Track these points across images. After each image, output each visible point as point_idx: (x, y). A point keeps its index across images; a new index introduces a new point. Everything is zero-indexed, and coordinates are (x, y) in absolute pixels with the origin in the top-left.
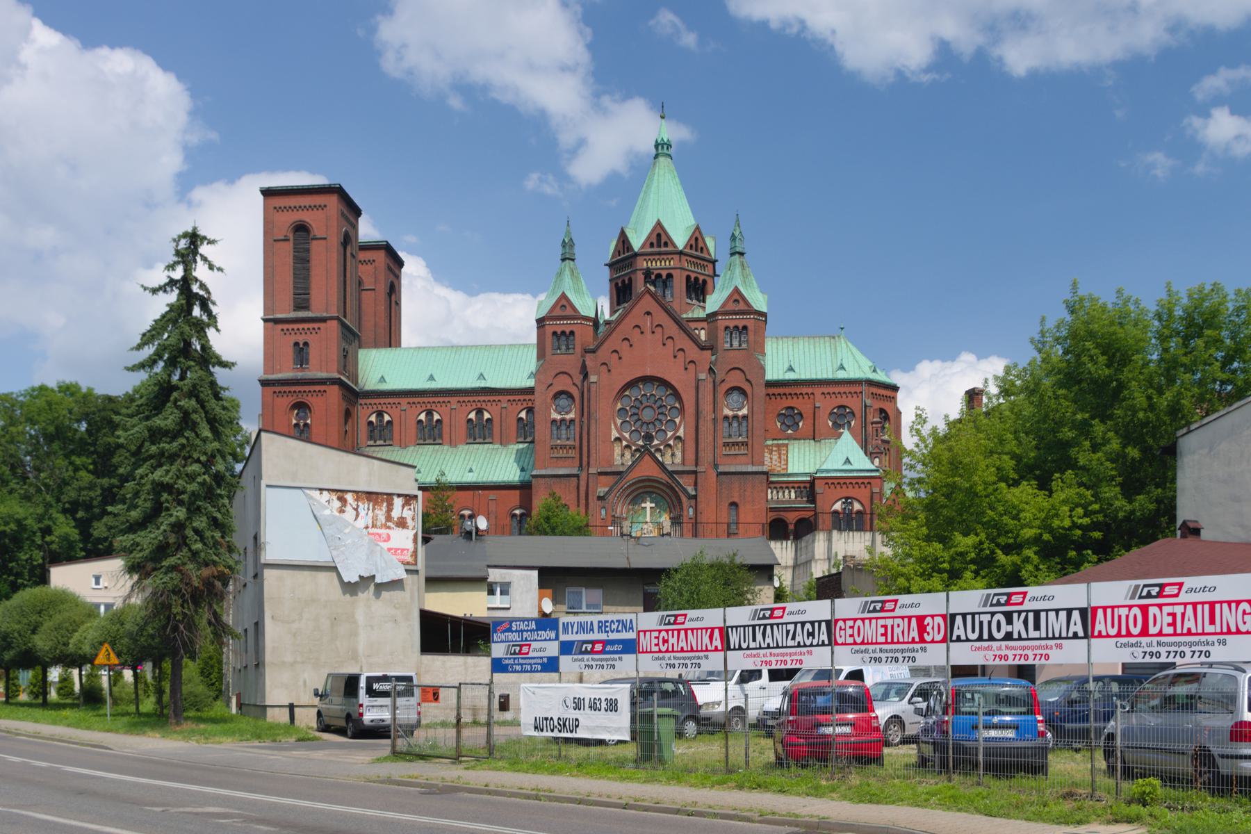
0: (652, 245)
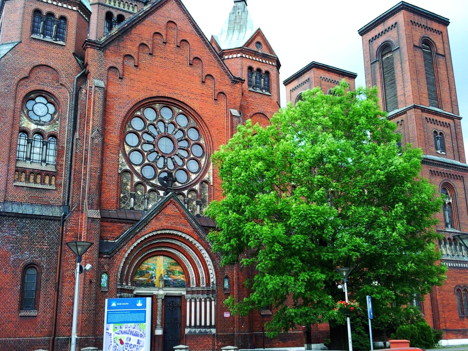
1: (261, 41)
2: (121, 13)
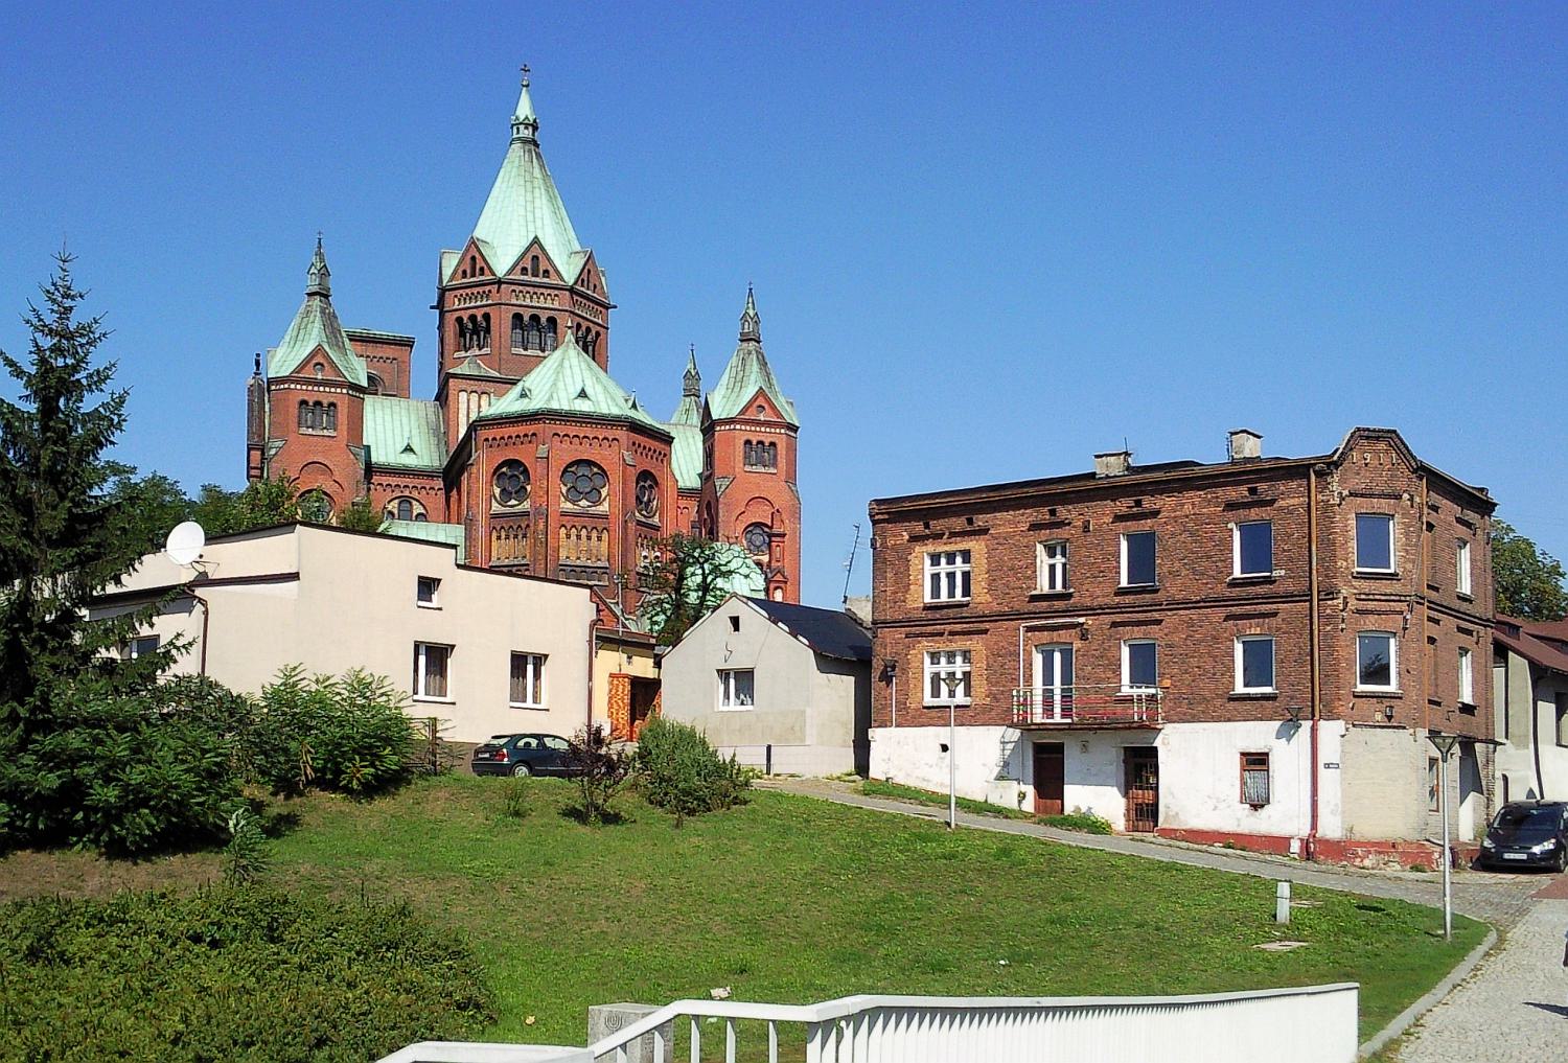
0: (524, 271)
2: (535, 311)
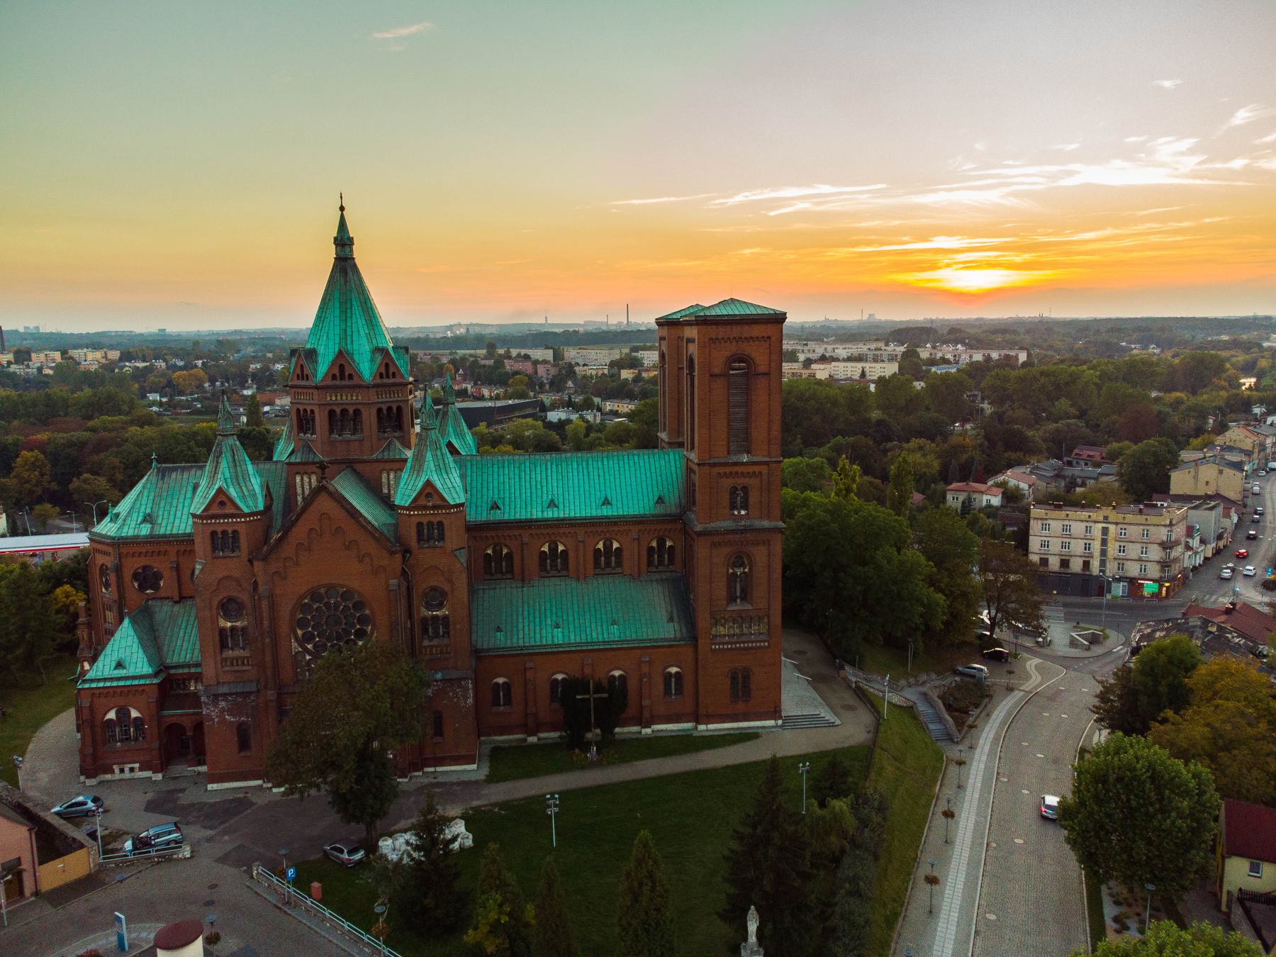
0: (334, 377)
1: (432, 491)
2: (344, 407)
